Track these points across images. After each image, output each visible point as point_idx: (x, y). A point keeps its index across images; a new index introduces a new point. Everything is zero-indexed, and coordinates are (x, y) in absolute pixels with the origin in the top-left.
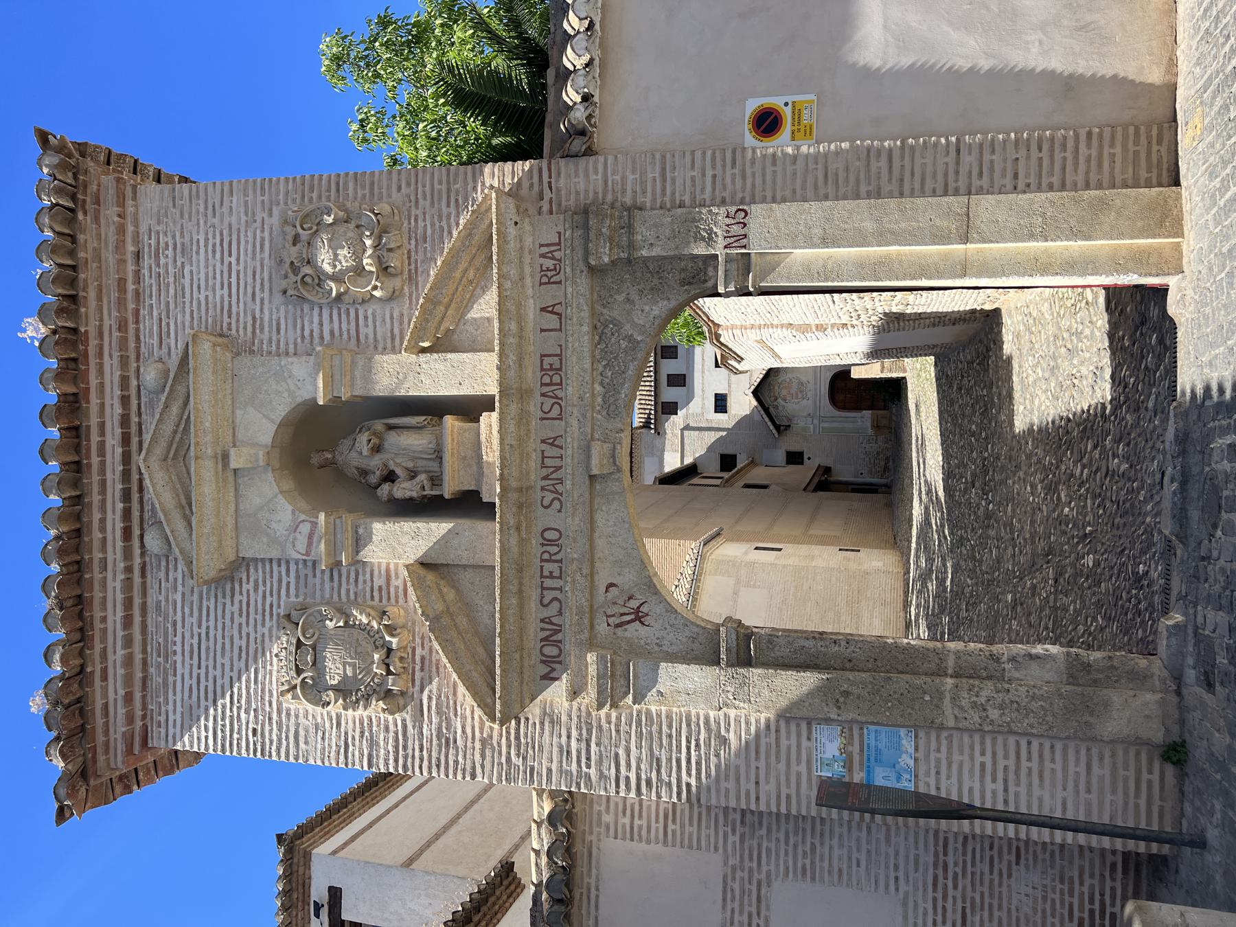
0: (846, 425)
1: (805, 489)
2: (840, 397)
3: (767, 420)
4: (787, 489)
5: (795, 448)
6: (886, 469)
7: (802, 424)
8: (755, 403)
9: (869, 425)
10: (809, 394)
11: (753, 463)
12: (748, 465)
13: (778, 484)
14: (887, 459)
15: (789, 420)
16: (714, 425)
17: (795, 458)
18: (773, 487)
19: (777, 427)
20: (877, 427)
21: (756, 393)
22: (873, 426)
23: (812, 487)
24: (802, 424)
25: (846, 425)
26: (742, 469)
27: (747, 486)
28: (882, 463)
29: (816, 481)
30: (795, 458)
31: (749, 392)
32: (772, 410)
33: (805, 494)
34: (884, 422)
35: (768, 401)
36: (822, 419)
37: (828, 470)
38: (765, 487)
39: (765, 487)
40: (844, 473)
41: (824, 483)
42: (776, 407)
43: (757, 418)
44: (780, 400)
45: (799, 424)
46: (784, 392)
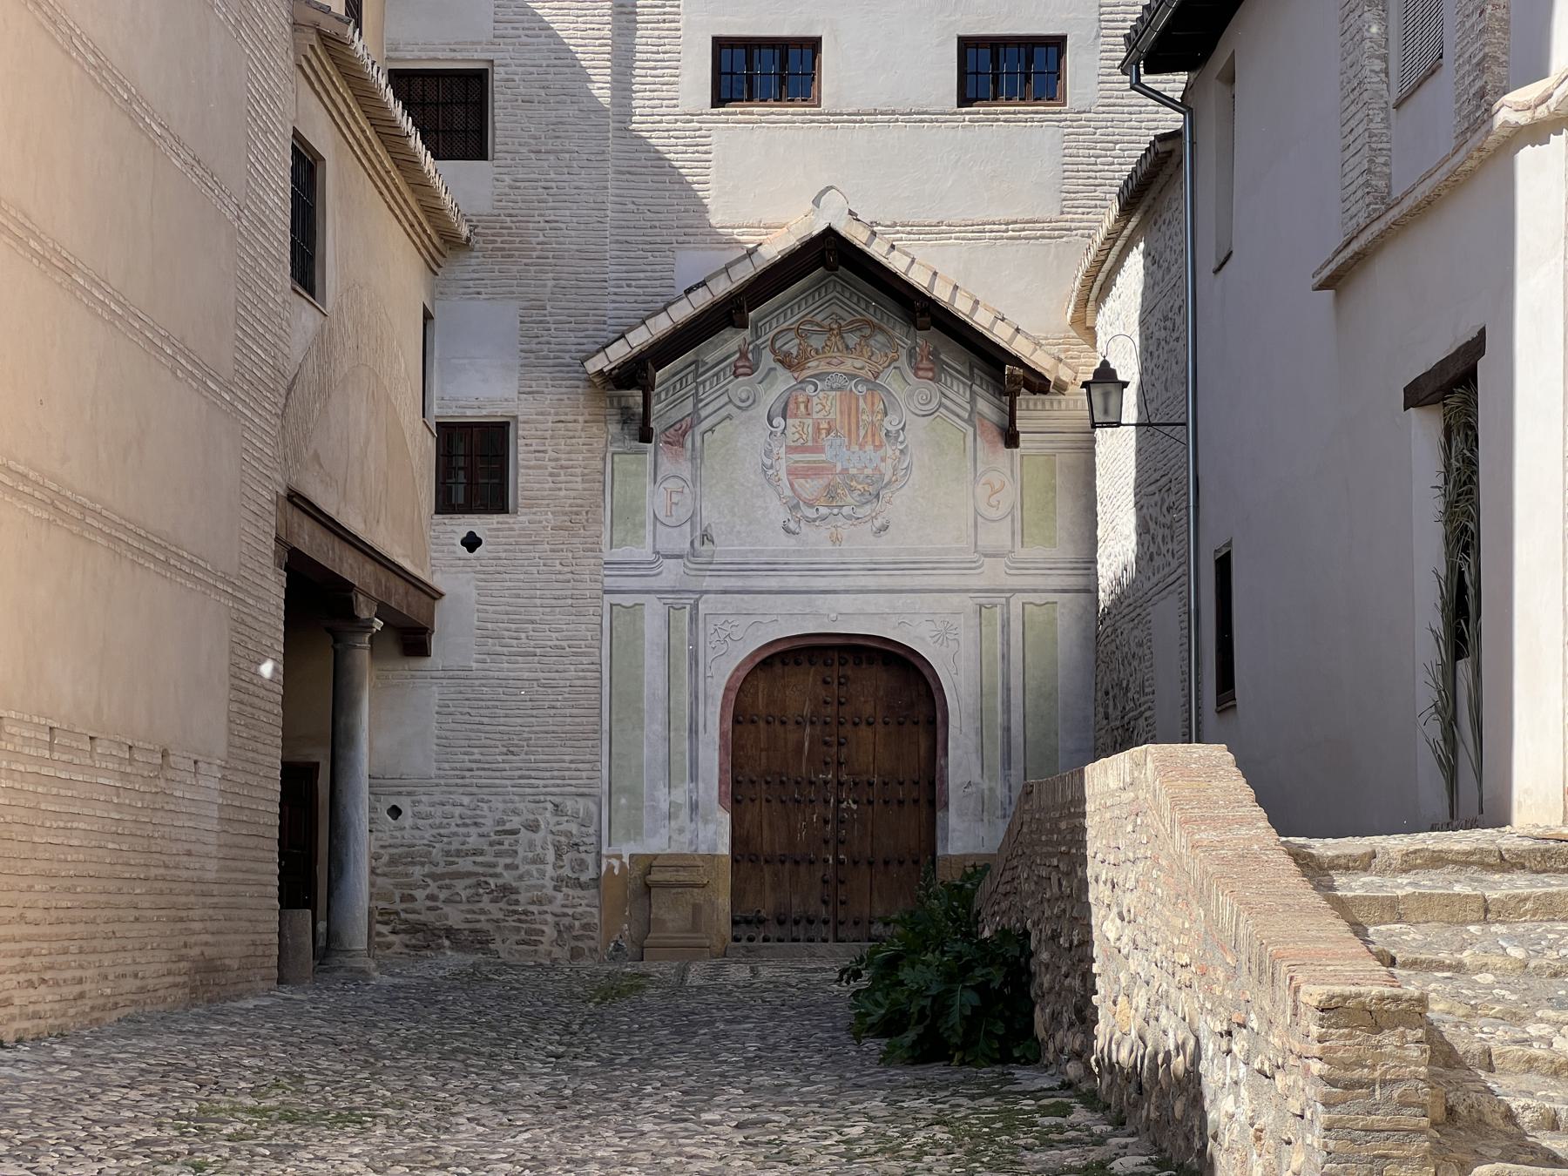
0: (654, 728)
1: (296, 500)
2: (801, 691)
3: (683, 312)
4: (296, 400)
5: (528, 469)
6: (425, 937)
7: (656, 499)
8: (775, 247)
9: (656, 844)
10: (816, 538)
11: (443, 243)
12: (433, 211)
13: (323, 344)
14: (479, 941)
15: (679, 435)
16: (645, 36)
17: (473, 466)
18: (305, 317)
19: (634, 374)
20: (648, 882)
21: (830, 257)
22: (648, 863)
23: (310, 540)
24: (656, 499)
25: (654, 728)
26: (420, 185)
27: (306, 168)
28: (455, 917)
29: (348, 566)
30: (473, 466)
31: (832, 216)
32: (731, 342)
33: (267, 495)
34: (671, 915)
35: (777, 319)
36: (684, 605)
37: (412, 639)
38: (305, 269)
39: (305, 269)
40: (396, 724)
41: (336, 612)
42: (745, 365)
43: (690, 263)
44: (784, 381)
45: (657, 487)
46: (825, 404)
